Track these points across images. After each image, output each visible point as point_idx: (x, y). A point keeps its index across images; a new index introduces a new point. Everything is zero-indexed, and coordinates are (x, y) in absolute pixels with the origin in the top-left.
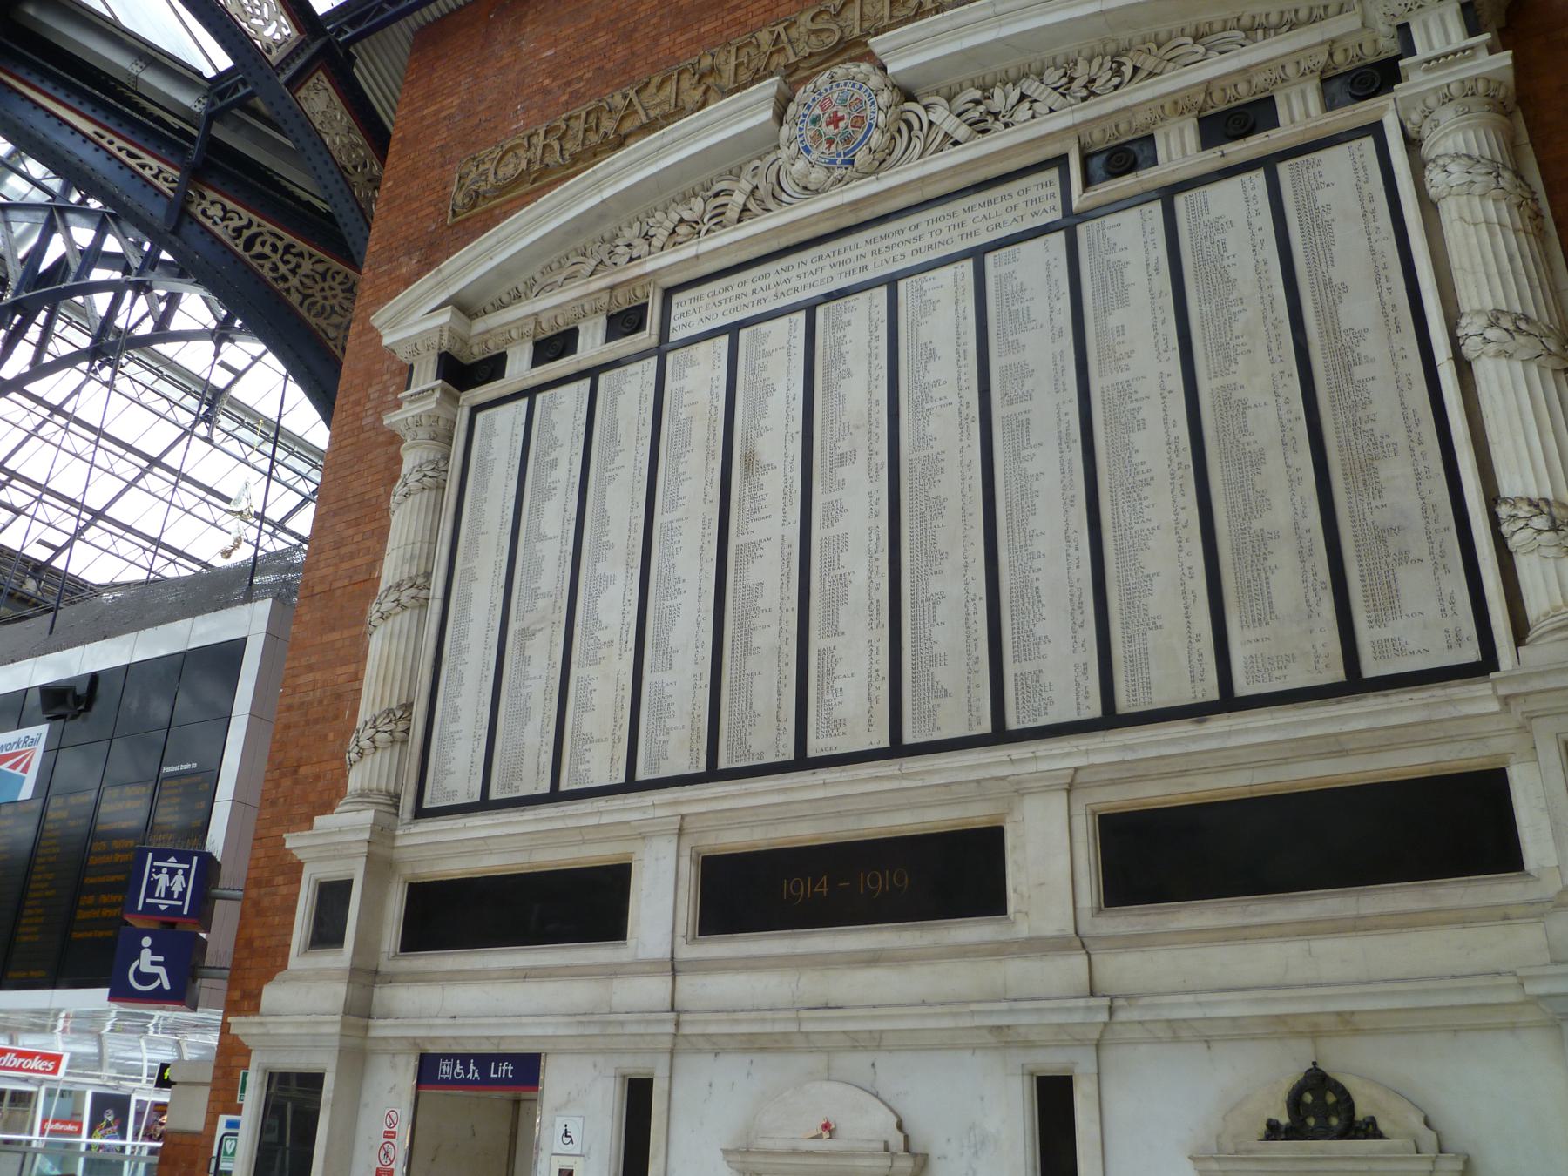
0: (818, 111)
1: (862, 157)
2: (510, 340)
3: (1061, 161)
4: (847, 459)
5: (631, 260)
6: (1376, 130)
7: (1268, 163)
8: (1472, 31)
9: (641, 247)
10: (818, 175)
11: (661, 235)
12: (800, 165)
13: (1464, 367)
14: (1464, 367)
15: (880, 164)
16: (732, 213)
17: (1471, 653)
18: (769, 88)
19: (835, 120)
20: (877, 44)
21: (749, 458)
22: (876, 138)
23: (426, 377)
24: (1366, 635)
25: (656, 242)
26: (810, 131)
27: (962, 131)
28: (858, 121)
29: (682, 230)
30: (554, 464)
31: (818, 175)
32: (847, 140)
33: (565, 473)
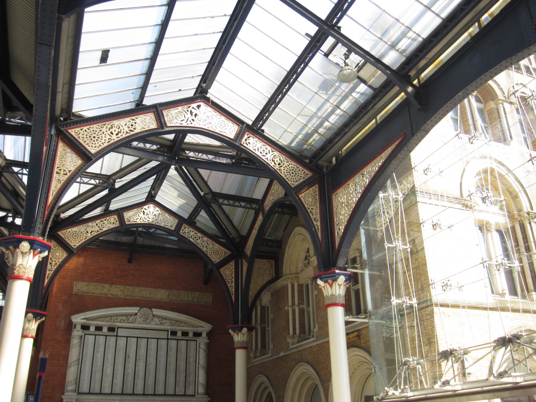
0: (143, 313)
1: (147, 322)
2: (92, 325)
3: (168, 331)
4: (141, 360)
5: (114, 321)
6: (196, 341)
7: (187, 340)
8: (207, 336)
9: (116, 321)
10: (142, 322)
11: (119, 320)
12: (139, 320)
13: (198, 368)
14: (198, 368)
15: (149, 324)
16: (129, 321)
17: (193, 394)
18: (139, 308)
19: (145, 316)
20: (153, 310)
21: (129, 356)
22: (149, 320)
23: (79, 327)
24: (187, 391)
25: (118, 321)
26: (142, 315)
27: (159, 324)
28: (148, 317)
29: (122, 321)
30: (100, 348)
31: (142, 322)
32: (146, 318)
33: (102, 349)
